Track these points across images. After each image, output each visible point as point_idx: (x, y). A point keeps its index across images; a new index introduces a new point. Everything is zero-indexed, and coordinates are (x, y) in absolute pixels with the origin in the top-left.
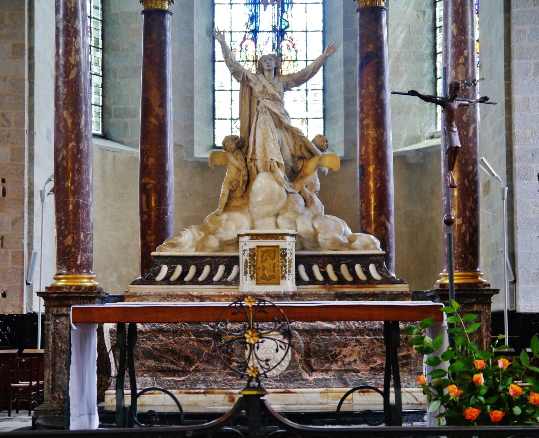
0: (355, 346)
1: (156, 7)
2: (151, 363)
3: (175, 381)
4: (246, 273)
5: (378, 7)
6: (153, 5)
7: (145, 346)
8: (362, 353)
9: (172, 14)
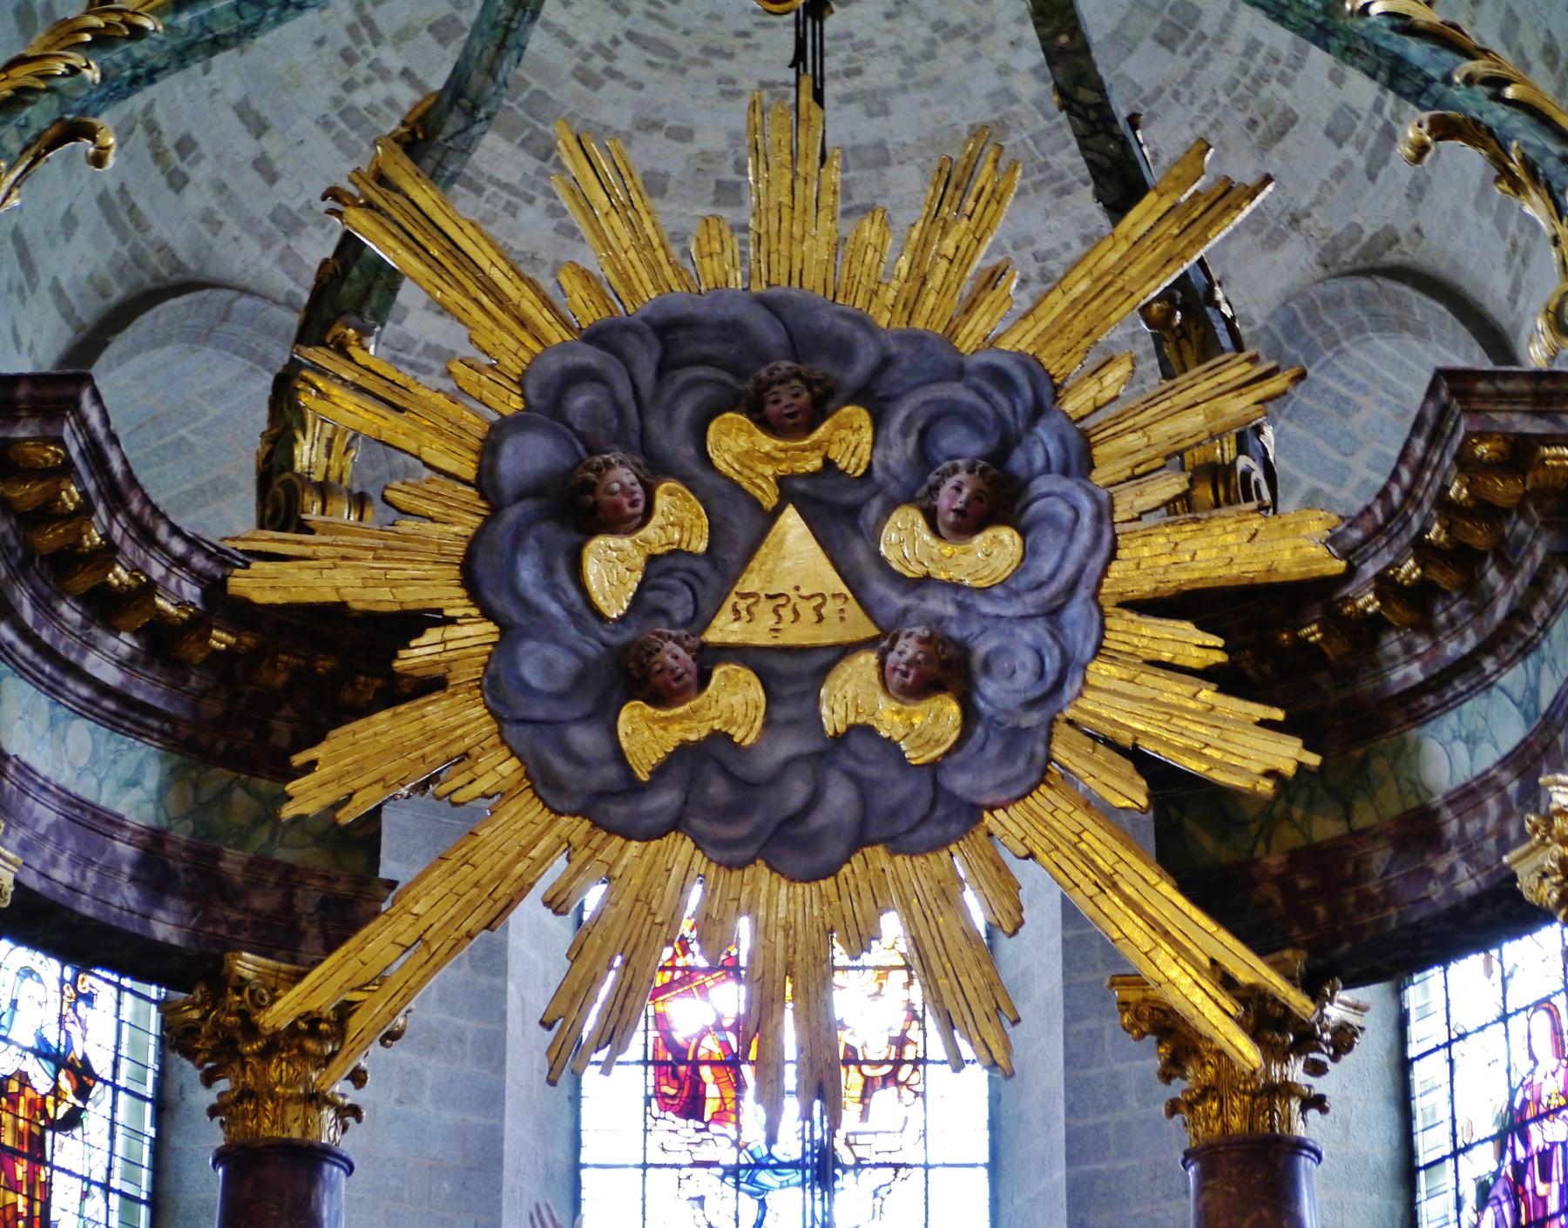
1: (277, 1133)
5: (1279, 1140)
6: (267, 1123)
9: (350, 1169)
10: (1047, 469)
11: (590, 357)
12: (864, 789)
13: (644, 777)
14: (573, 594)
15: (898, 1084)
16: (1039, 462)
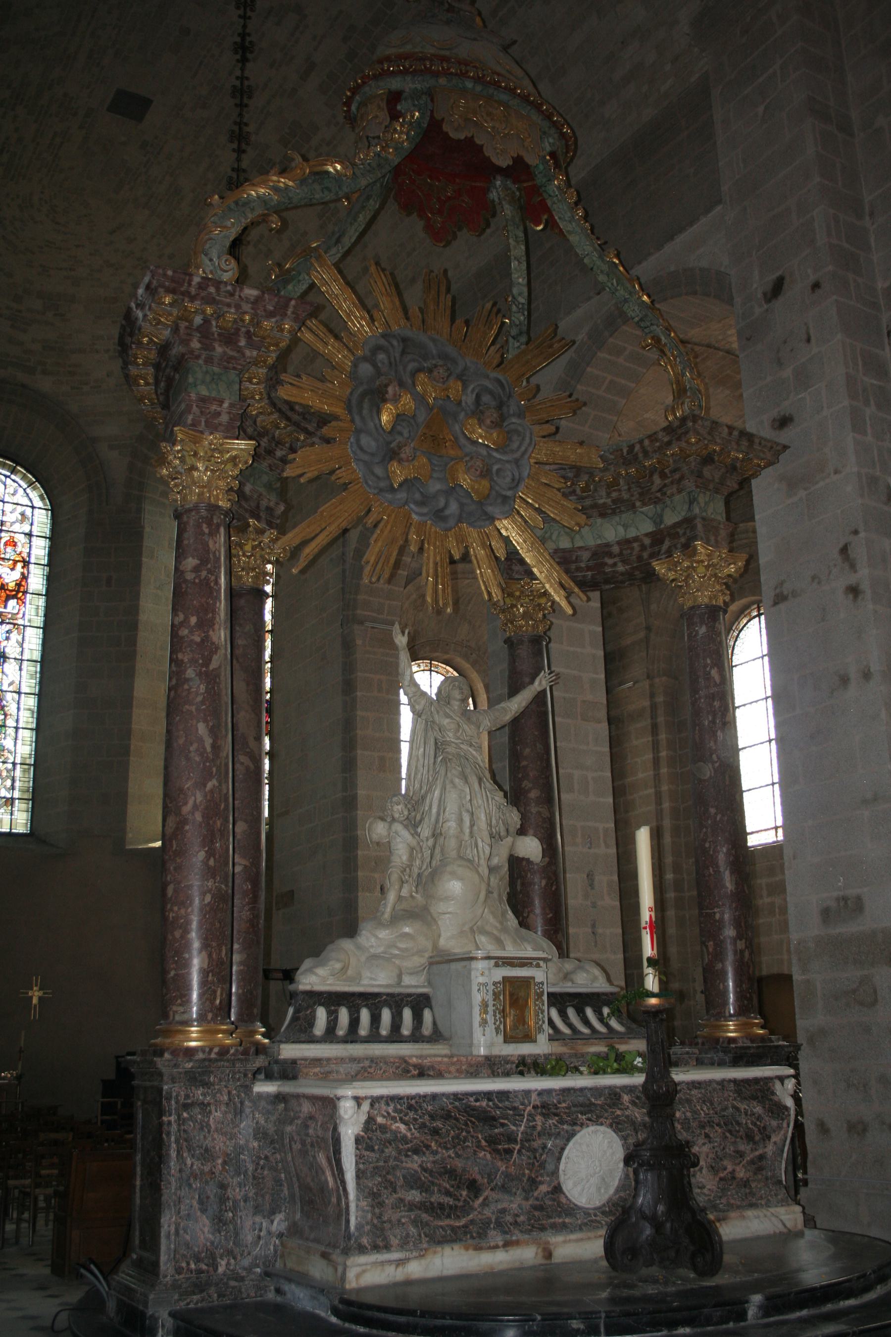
0: (704, 1144)
2: (414, 1196)
3: (453, 1229)
4: (484, 1022)
7: (409, 1165)
8: (711, 1155)
10: (514, 415)
11: (382, 342)
12: (462, 505)
13: (396, 486)
14: (377, 422)
15: (18, 599)
16: (511, 412)
